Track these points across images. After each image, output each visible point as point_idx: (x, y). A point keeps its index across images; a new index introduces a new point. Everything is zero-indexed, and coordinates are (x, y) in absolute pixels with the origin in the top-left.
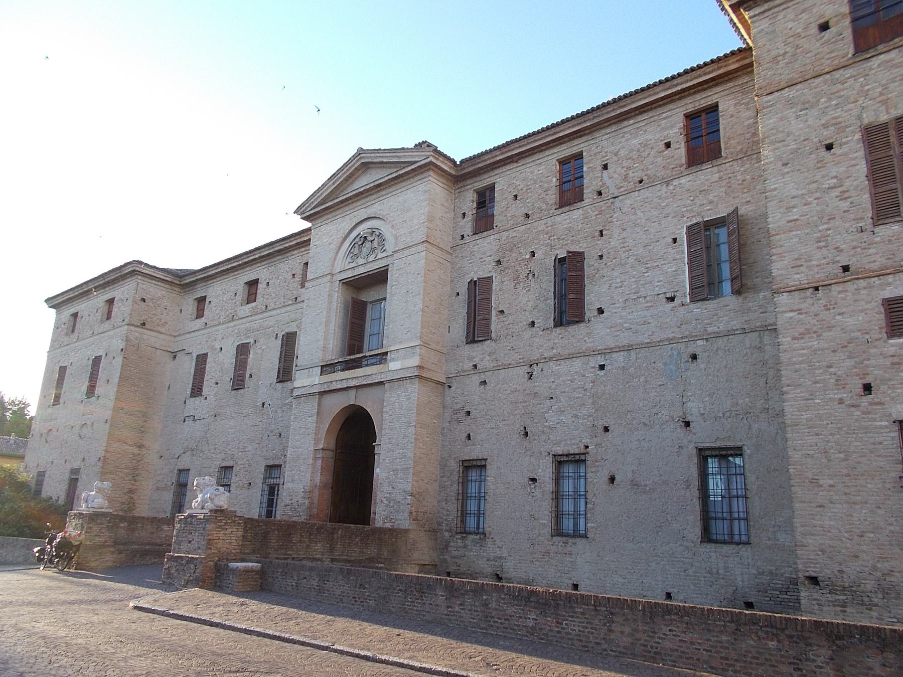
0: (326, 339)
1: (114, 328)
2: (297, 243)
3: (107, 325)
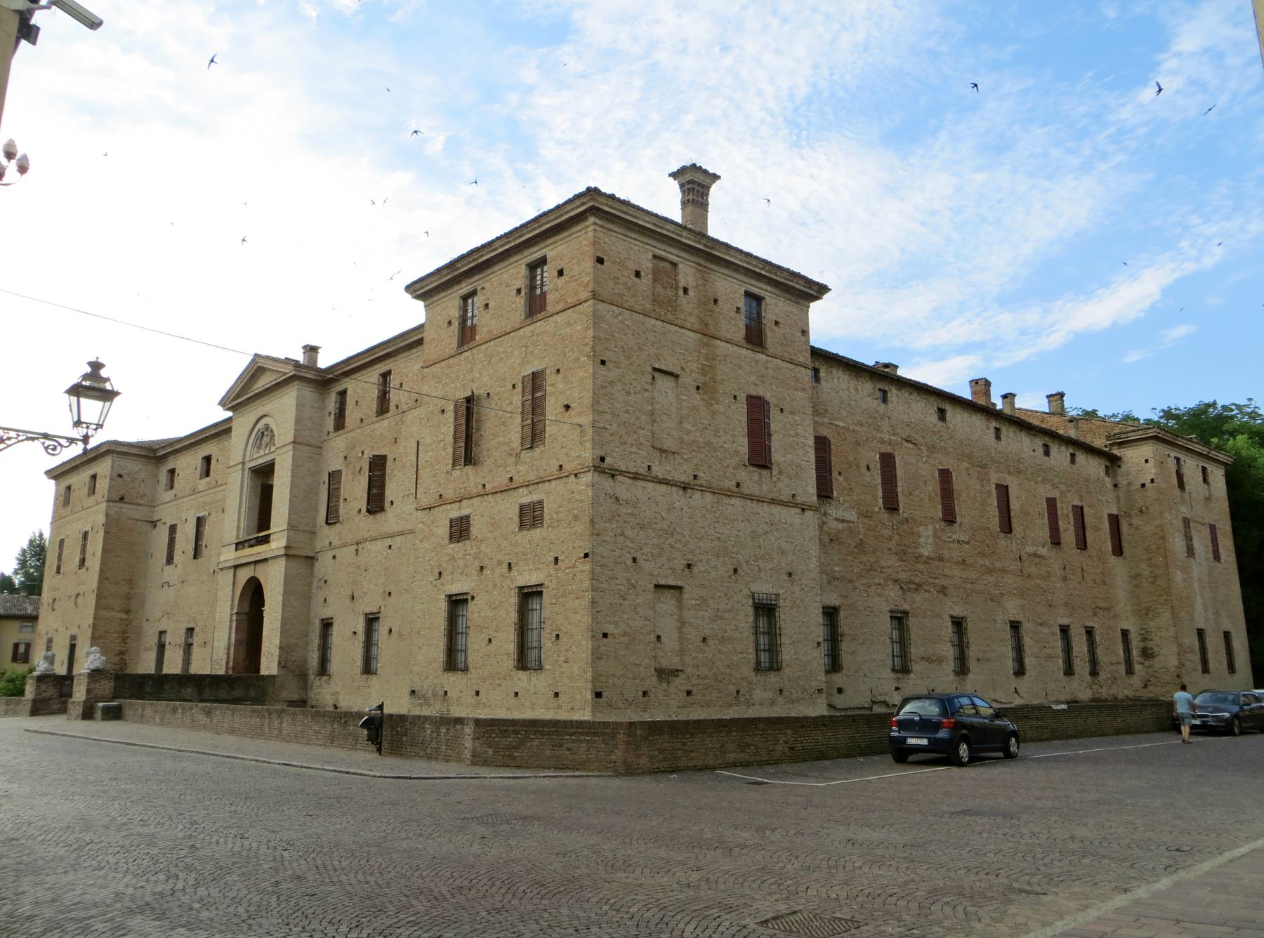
0: (239, 520)
1: (97, 504)
2: (219, 432)
3: (92, 499)
